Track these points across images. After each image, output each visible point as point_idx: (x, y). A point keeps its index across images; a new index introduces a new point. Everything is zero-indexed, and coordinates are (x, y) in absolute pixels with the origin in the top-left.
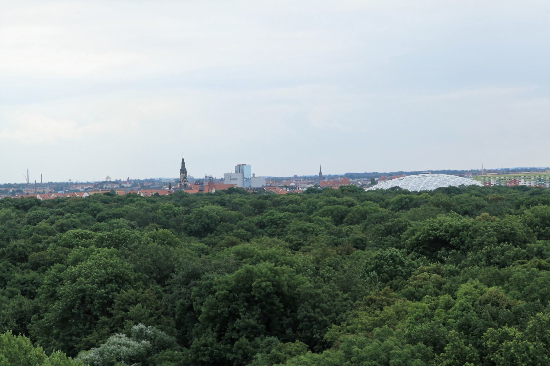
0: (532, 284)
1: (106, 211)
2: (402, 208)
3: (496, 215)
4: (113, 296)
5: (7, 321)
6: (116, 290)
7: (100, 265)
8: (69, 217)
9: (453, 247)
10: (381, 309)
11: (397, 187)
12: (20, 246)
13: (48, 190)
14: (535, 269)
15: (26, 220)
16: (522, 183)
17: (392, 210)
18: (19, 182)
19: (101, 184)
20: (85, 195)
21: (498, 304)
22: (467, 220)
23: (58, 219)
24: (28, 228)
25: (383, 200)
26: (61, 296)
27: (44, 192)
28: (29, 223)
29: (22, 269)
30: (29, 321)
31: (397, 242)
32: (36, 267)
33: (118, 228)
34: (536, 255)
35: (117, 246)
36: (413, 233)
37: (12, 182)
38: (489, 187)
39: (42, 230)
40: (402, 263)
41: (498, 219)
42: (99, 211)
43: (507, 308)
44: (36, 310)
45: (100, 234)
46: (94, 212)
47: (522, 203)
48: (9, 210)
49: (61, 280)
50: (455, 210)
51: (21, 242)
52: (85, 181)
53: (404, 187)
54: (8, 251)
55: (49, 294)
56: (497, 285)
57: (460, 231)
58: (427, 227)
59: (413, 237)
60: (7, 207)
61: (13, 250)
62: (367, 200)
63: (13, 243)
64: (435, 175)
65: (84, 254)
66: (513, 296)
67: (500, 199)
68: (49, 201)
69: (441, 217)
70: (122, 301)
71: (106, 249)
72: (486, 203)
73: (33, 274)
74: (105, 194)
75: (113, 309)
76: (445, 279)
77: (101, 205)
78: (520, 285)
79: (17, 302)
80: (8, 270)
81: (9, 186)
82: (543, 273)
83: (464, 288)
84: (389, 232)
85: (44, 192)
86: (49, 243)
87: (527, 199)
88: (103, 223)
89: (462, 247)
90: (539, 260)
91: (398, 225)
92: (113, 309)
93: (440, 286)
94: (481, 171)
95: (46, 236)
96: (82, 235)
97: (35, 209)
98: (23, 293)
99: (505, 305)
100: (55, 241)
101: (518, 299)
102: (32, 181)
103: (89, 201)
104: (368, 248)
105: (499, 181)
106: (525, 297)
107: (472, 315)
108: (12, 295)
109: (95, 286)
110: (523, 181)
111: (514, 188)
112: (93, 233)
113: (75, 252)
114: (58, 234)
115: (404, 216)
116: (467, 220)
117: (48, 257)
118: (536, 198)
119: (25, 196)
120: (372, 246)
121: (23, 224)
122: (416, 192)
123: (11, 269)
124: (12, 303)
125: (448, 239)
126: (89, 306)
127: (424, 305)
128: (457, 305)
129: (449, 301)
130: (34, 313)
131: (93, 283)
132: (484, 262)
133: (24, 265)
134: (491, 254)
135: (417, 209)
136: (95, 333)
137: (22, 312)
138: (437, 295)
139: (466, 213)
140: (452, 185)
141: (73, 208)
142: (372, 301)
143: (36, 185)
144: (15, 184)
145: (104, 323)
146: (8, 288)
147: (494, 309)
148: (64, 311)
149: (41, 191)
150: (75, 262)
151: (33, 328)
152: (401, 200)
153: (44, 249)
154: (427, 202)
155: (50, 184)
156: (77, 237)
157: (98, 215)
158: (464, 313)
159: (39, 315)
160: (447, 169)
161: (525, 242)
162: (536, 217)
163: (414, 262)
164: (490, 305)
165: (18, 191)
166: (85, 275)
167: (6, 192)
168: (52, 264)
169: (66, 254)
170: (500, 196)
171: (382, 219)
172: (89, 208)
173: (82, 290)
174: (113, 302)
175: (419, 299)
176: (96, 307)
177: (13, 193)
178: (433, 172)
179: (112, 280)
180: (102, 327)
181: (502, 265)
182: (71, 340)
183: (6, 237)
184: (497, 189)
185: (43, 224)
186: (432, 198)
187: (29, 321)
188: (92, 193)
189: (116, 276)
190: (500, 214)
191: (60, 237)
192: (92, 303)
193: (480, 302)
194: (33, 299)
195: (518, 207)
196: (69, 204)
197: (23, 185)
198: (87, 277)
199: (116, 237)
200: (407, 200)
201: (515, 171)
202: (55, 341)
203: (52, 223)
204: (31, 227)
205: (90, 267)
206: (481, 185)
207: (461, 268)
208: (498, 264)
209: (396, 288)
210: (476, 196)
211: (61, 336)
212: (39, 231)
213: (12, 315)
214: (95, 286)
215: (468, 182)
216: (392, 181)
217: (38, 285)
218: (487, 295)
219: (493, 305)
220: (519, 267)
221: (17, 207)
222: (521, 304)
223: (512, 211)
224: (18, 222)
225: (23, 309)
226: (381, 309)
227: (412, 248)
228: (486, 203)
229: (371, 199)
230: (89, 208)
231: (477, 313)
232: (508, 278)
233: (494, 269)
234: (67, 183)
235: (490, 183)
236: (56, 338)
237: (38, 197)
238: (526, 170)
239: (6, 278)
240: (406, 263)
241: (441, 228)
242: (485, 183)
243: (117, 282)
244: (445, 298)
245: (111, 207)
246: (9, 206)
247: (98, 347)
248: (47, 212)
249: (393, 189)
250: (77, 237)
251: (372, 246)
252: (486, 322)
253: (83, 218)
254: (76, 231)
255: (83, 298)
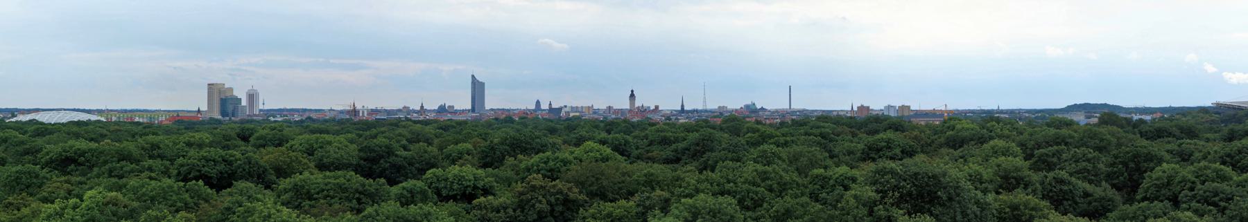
0: (144, 189)
2: (38, 135)
3: (116, 142)
9: (80, 164)
10: (19, 210)
11: (34, 120)
14: (147, 180)
16: (137, 119)
17: (30, 136)
21: (116, 205)
22: (94, 145)
25: (22, 129)
31: (33, 160)
34: (147, 170)
36: (47, 154)
38: (111, 122)
40: (37, 176)
41: (117, 144)
43: (124, 207)
47: (137, 134)
50: (83, 138)
53: (40, 120)
56: (116, 191)
57: (85, 153)
58: (60, 149)
59: (48, 157)
62: (8, 129)
64: (67, 112)
66: (130, 199)
67: (120, 130)
69: (71, 142)
72: (108, 133)
76: (74, 187)
78: (135, 190)
82: (153, 182)
83: (90, 193)
84: (27, 153)
87: (141, 131)
89: (87, 164)
90: (149, 173)
91: (34, 148)
93: (69, 192)
94: (104, 111)
99: (122, 206)
101: (133, 201)
104: (7, 164)
105: (119, 118)
106: (138, 199)
107: (96, 213)
110: (137, 118)
111: (130, 123)
115: (39, 141)
116: (94, 145)
118: (147, 130)
120: (11, 163)
122: (51, 124)
125: (77, 158)
127: (57, 206)
128: (83, 206)
129: (76, 203)
132: (106, 175)
134: (112, 169)
135: (51, 136)
138: (67, 199)
139: (91, 140)
140: (81, 120)
142: (11, 204)
147: (114, 208)
152: (38, 129)
154: (59, 131)
158: (89, 212)
160: (76, 108)
161: (139, 161)
162: (147, 144)
163: (48, 176)
164: (111, 205)
170: (118, 128)
171: (22, 143)
175: (52, 202)
178: (65, 110)
181: (121, 177)
184: (116, 123)
186: (64, 128)
190: (119, 141)
193: (103, 203)
195: (133, 137)
200: (43, 129)
201: (131, 111)
206: (105, 120)
207: (88, 179)
208: (117, 176)
209: (31, 195)
210: (100, 127)
215: (94, 118)
216: (30, 115)
218: (108, 199)
219: (113, 205)
220: (135, 179)
222: (135, 204)
223: (129, 139)
226: (19, 210)
227: (47, 164)
228: (108, 133)
229: (11, 129)
231: (99, 211)
232: (125, 186)
233: (114, 180)
235: (111, 119)
238: (140, 111)
240: (41, 175)
241: (71, 151)
242: (107, 119)
244: (73, 201)
249: (30, 121)
251: (11, 163)
252: (108, 218)
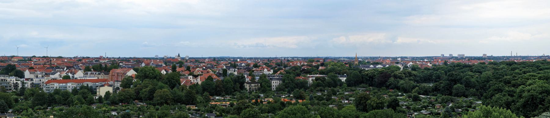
1: (542, 67)
4: (545, 98)
5: (502, 105)
6: (546, 96)
7: (540, 86)
8: (527, 69)
12: (508, 78)
13: (519, 58)
15: (510, 69)
18: (508, 56)
19: (541, 57)
20: (534, 61)
23: (523, 69)
24: (511, 72)
26: (524, 97)
27: (518, 59)
28: (512, 70)
29: (509, 86)
30: (511, 105)
32: (514, 86)
33: (547, 73)
35: (547, 80)
37: (505, 56)
39: (516, 73)
42: (540, 66)
44: (513, 101)
45: (540, 75)
46: (538, 67)
48: (504, 65)
49: (524, 91)
51: (509, 77)
52: (534, 56)
54: (503, 80)
55: (519, 96)
60: (503, 64)
61: (505, 79)
63: (505, 77)
65: (533, 82)
68: (519, 62)
70: (549, 100)
71: (542, 81)
73: (513, 88)
74: (542, 60)
75: (545, 103)
77: (540, 65)
79: (506, 98)
80: (503, 87)
81: (504, 57)
85: (518, 59)
86: (519, 77)
88: (541, 71)
92: (545, 103)
95: (518, 75)
96: (532, 75)
97: (514, 65)
98: (509, 95)
100: (522, 77)
102: (513, 55)
103: (536, 63)
108: (504, 95)
109: (538, 94)
112: (537, 75)
113: (530, 81)
114: (523, 75)
117: (519, 83)
119: (510, 61)
121: (509, 71)
123: (504, 86)
124: (504, 98)
126: (535, 101)
130: (513, 102)
131: (537, 93)
133: (509, 85)
136: (537, 111)
137: (508, 102)
141: (529, 65)
143: (515, 57)
144: (507, 56)
145: (541, 108)
146: (503, 93)
148: (525, 102)
149: (517, 59)
150: (530, 85)
151: (513, 107)
153: (517, 80)
155: (520, 57)
156: (530, 76)
157: (539, 68)
159: (515, 103)
165: (507, 59)
166: (534, 90)
167: (503, 59)
168: (520, 85)
169: (526, 82)
172: (535, 65)
173: (532, 95)
174: (545, 100)
176: (538, 102)
177: (506, 59)
179: (544, 92)
180: (540, 109)
182: (527, 113)
183: (502, 75)
185: (517, 71)
187: (511, 105)
188: (537, 60)
189: (546, 91)
191: (524, 76)
192: (536, 100)
194: (512, 97)
196: (528, 63)
197: (509, 57)
198: (534, 90)
199: (546, 76)
202: (520, 113)
203: (521, 70)
204: (512, 72)
205: (536, 87)
211: (523, 111)
212: (516, 73)
213: (504, 103)
214: (538, 94)
217: (515, 92)
221: (507, 64)
224: (507, 70)
225: (509, 101)
230: (535, 65)
234: (527, 56)
236: (521, 112)
237: (515, 61)
239: (502, 89)
243: (546, 93)
245: (545, 65)
246: (504, 64)
247: (538, 116)
248: (519, 66)
250: (530, 76)
253: (533, 69)
254: (530, 73)
255: (532, 98)
